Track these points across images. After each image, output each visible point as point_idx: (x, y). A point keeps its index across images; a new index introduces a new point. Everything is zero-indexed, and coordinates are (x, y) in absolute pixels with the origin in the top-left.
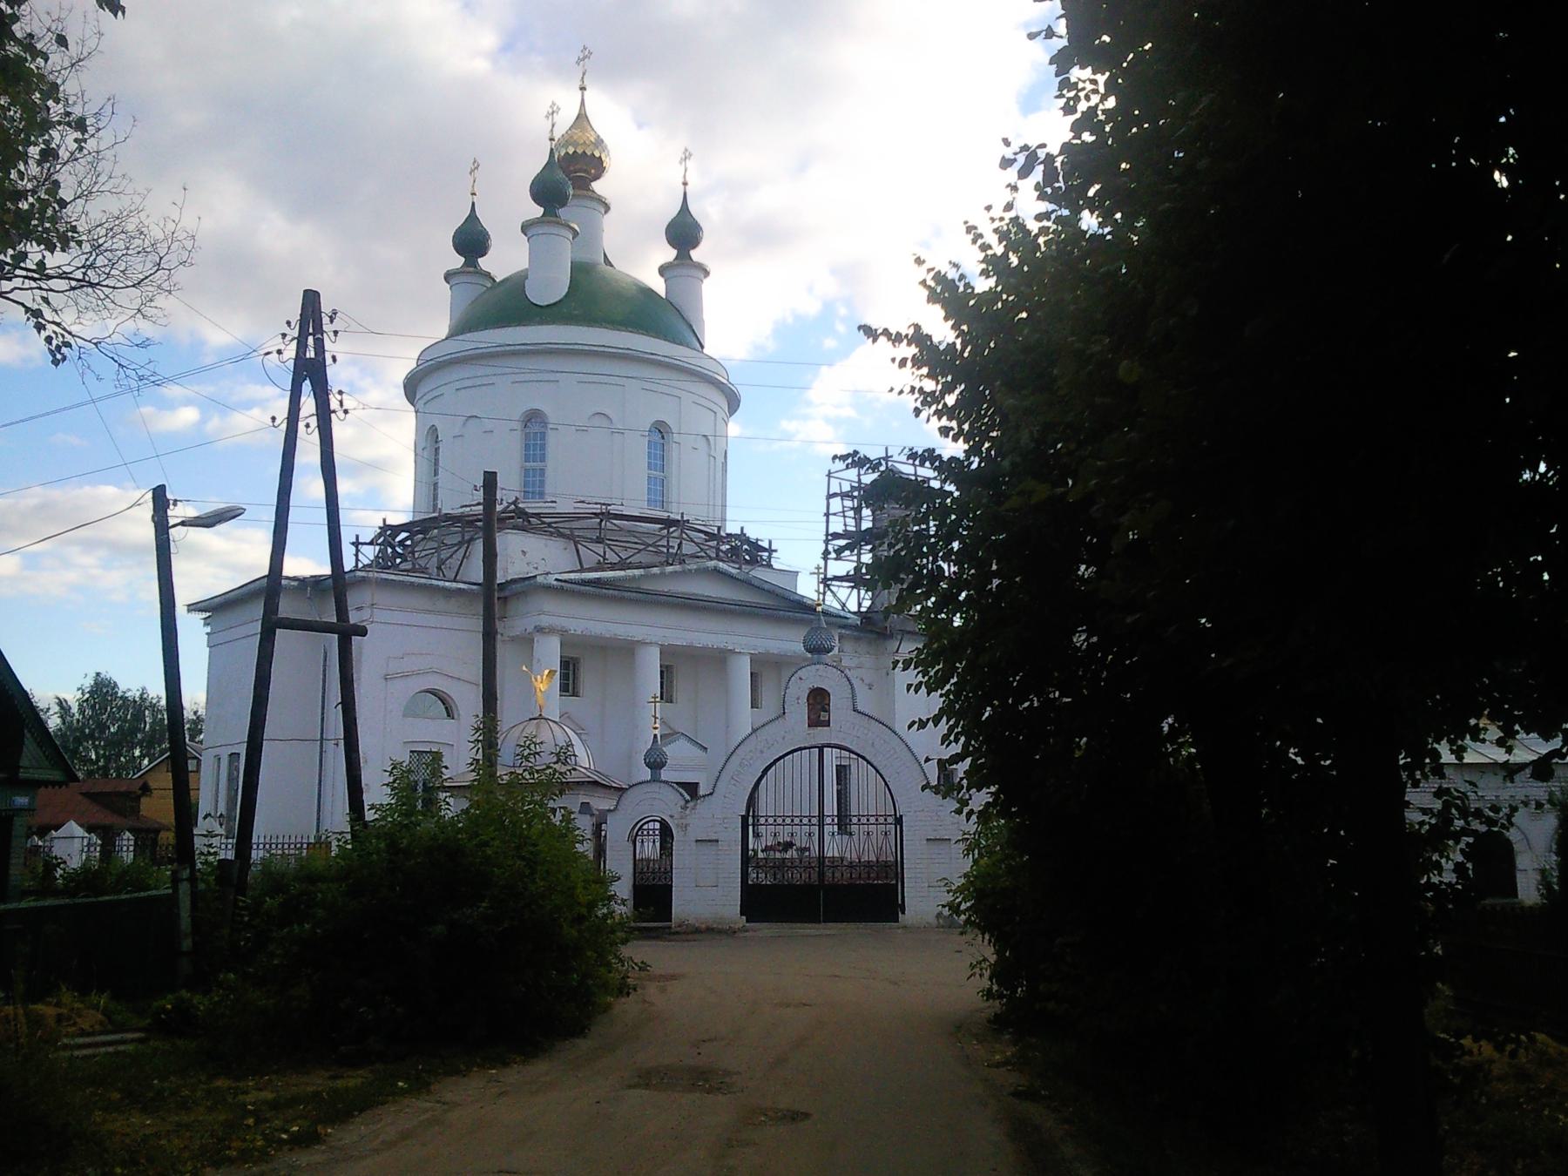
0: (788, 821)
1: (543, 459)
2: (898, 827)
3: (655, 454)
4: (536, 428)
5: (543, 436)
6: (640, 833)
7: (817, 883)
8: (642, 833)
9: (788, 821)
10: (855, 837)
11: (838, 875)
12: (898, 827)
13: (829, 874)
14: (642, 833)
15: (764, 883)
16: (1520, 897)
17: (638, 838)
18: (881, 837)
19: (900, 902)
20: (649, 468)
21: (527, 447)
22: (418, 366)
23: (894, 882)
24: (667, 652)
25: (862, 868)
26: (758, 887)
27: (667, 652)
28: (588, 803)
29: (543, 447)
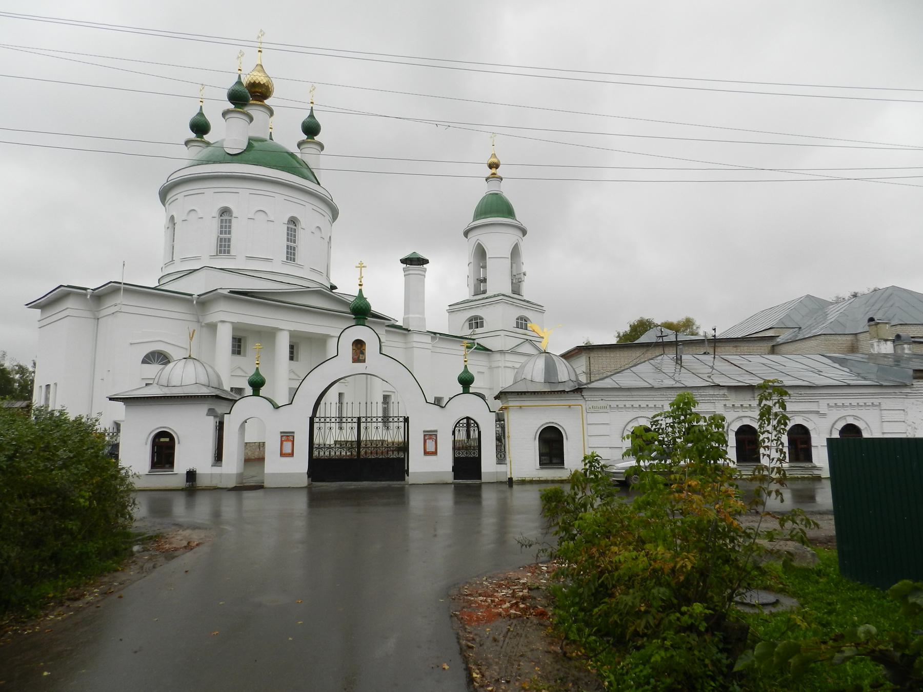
0: (374, 420)
1: (230, 233)
2: (406, 424)
3: (291, 234)
4: (225, 217)
5: (230, 221)
6: (458, 425)
7: (356, 458)
8: (459, 425)
9: (374, 420)
10: (344, 431)
11: (333, 453)
12: (406, 424)
13: (363, 452)
14: (459, 425)
15: (392, 457)
16: (761, 462)
17: (456, 428)
18: (349, 431)
19: (406, 468)
20: (288, 241)
21: (222, 227)
22: (167, 182)
23: (403, 457)
24: (236, 327)
25: (372, 449)
26: (459, 458)
27: (236, 327)
28: (214, 409)
29: (230, 227)
